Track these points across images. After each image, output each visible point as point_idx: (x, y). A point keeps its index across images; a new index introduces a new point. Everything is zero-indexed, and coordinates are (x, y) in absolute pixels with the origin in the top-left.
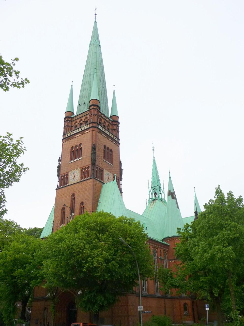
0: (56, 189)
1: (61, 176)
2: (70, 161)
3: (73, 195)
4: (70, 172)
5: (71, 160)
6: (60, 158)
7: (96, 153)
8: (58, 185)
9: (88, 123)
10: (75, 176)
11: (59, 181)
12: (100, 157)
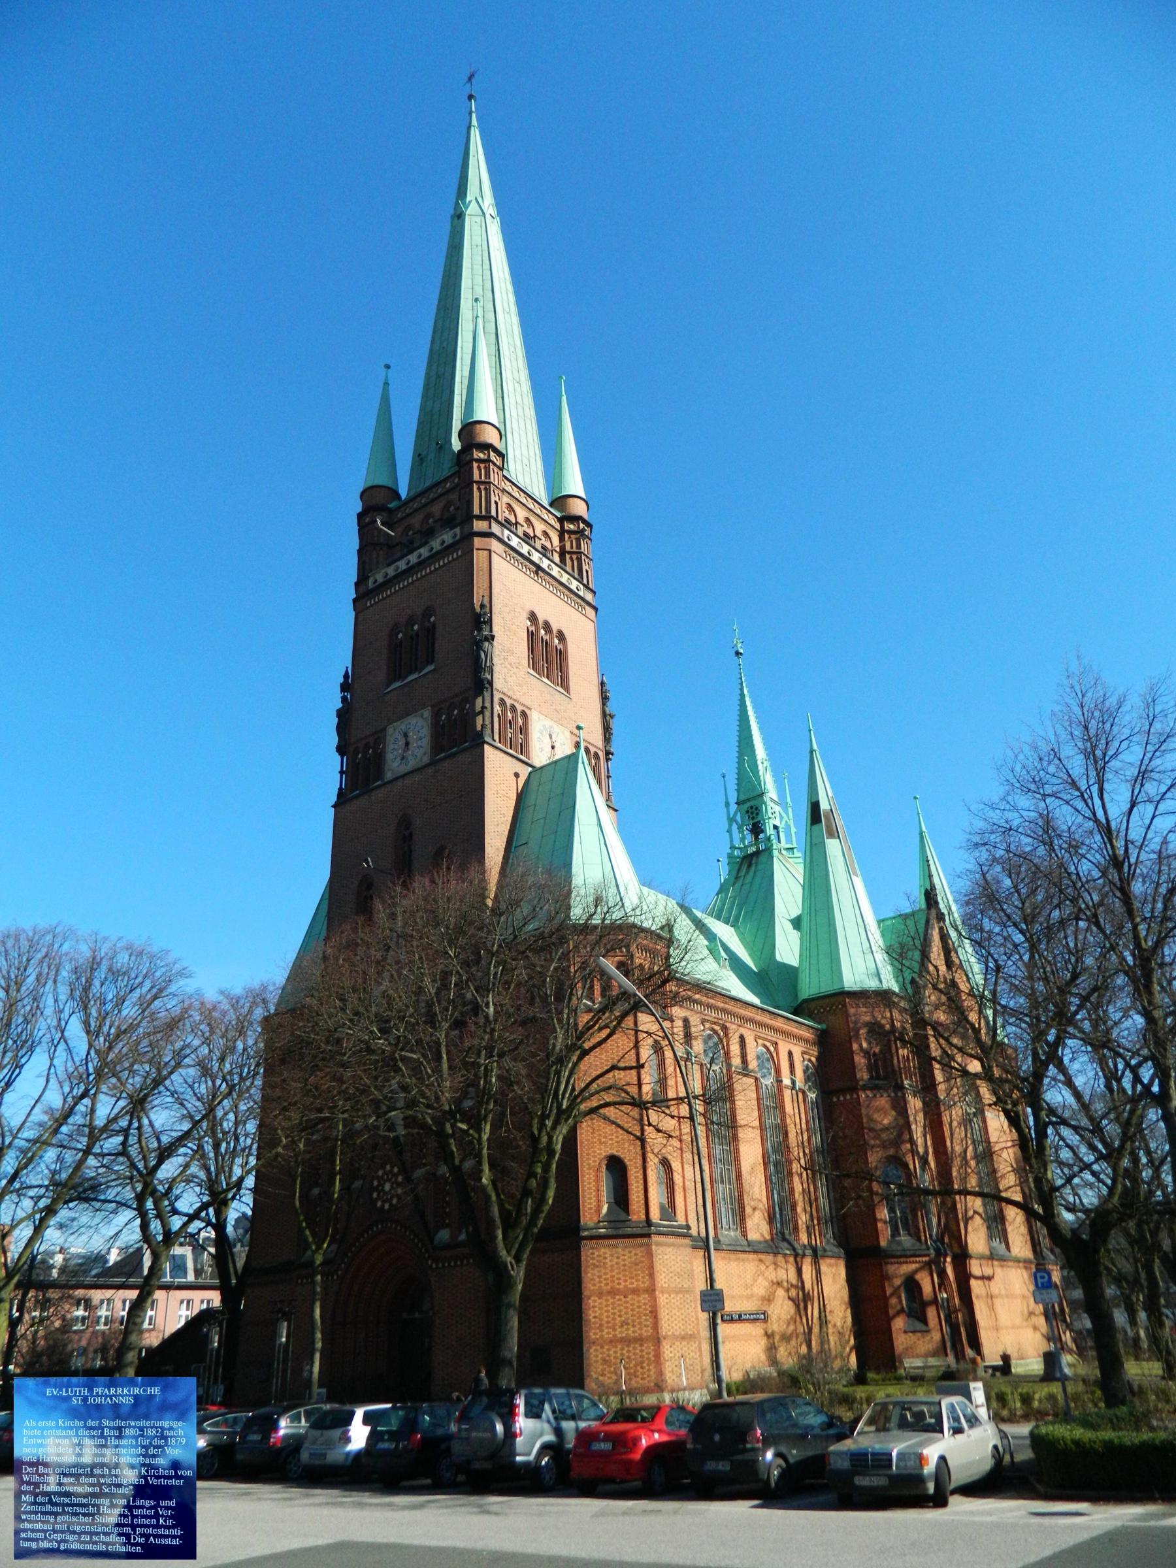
1: (351, 749)
2: (388, 686)
4: (390, 730)
6: (346, 676)
7: (493, 637)
9: (458, 520)
12: (511, 659)
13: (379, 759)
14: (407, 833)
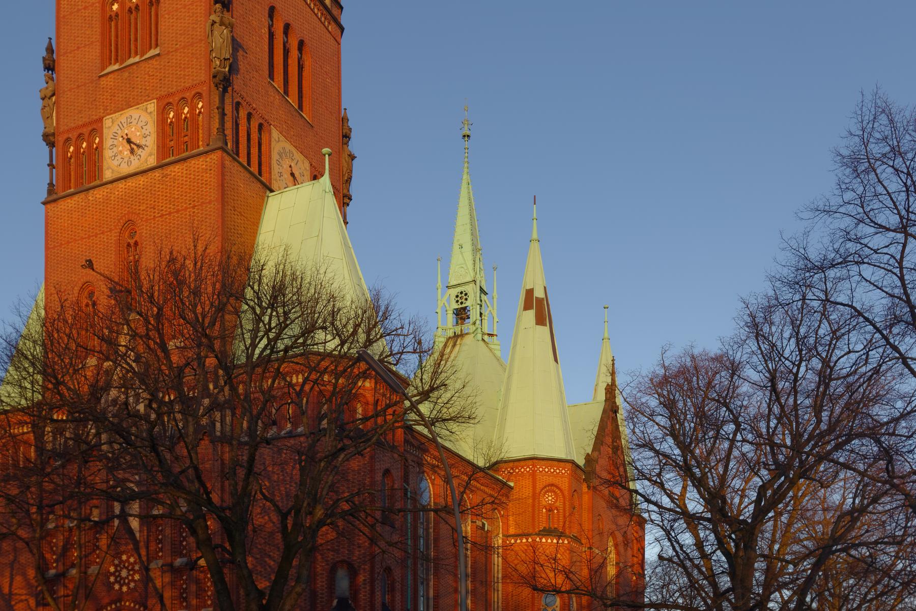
0: (44, 203)
2: (103, 69)
4: (107, 122)
5: (106, 61)
8: (51, 184)
10: (130, 138)
11: (54, 163)
13: (95, 156)
14: (132, 242)
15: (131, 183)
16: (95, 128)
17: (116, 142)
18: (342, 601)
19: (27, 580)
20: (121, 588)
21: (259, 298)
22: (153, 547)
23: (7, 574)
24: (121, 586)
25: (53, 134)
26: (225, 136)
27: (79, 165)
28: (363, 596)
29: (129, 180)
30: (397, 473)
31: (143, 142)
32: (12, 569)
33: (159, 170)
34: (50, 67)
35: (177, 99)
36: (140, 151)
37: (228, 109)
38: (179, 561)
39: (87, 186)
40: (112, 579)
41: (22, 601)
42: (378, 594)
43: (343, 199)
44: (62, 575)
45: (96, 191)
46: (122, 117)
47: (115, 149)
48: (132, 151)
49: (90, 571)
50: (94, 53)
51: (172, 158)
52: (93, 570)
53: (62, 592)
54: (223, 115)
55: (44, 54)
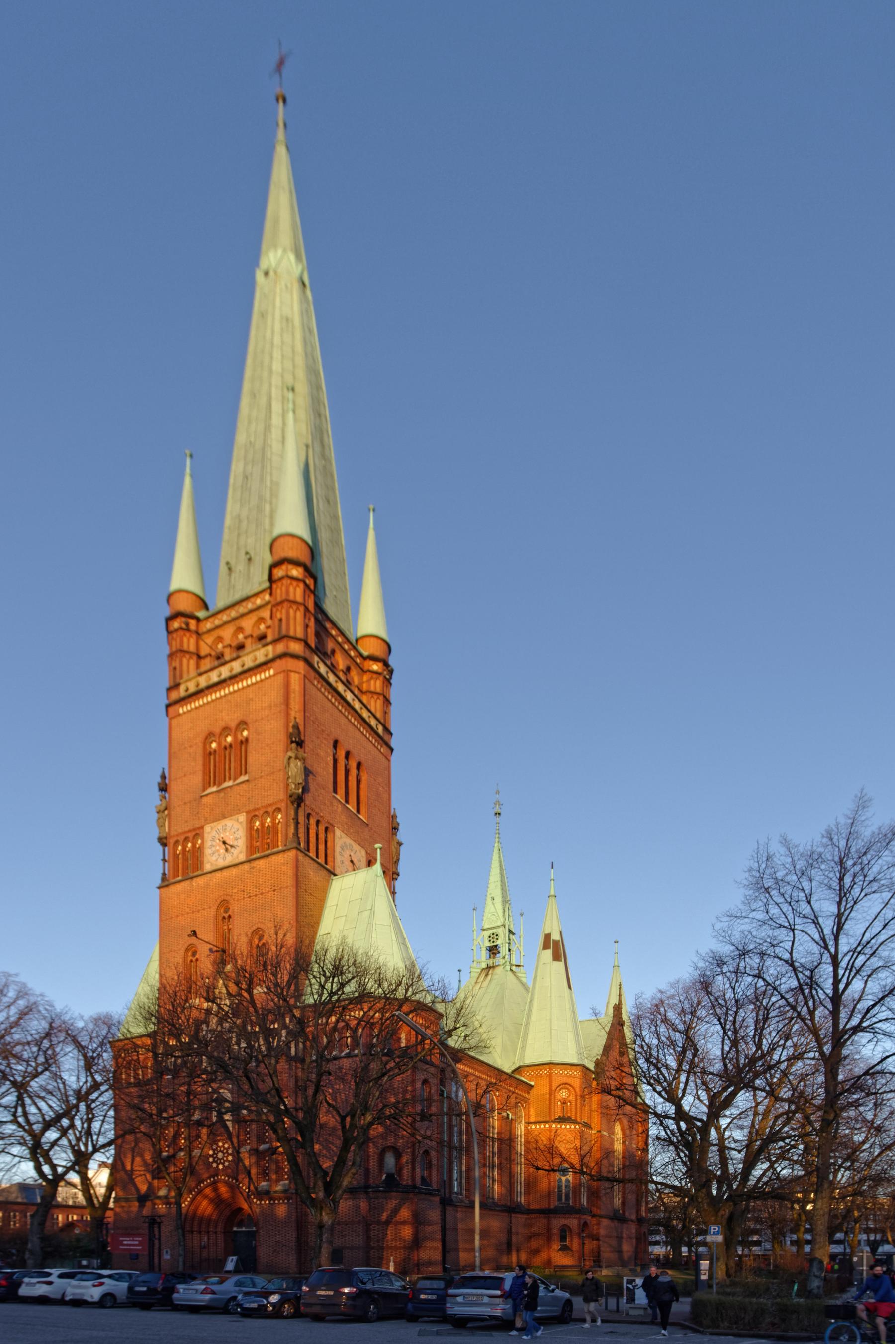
0: (159, 888)
3: (224, 904)
4: (207, 829)
5: (206, 784)
8: (164, 874)
11: (166, 858)
13: (197, 855)
14: (226, 915)
15: (225, 873)
16: (198, 833)
17: (214, 843)
18: (390, 1176)
19: (144, 1161)
20: (218, 1167)
21: (324, 971)
22: (242, 1137)
23: (130, 1156)
24: (218, 1165)
25: (166, 838)
26: (298, 838)
27: (186, 860)
28: (406, 1172)
29: (225, 871)
30: (434, 1081)
31: (235, 843)
32: (133, 1152)
33: (248, 864)
34: (163, 788)
35: (261, 812)
36: (232, 850)
37: (302, 819)
38: (262, 1147)
39: (192, 875)
40: (211, 1160)
41: (141, 1175)
42: (418, 1171)
43: (391, 874)
44: (173, 1156)
45: (198, 879)
46: (219, 825)
47: (213, 849)
48: (227, 850)
49: (194, 1154)
50: (197, 779)
51: (257, 855)
52: (196, 1153)
53: (172, 1169)
54: (297, 823)
55: (159, 780)
